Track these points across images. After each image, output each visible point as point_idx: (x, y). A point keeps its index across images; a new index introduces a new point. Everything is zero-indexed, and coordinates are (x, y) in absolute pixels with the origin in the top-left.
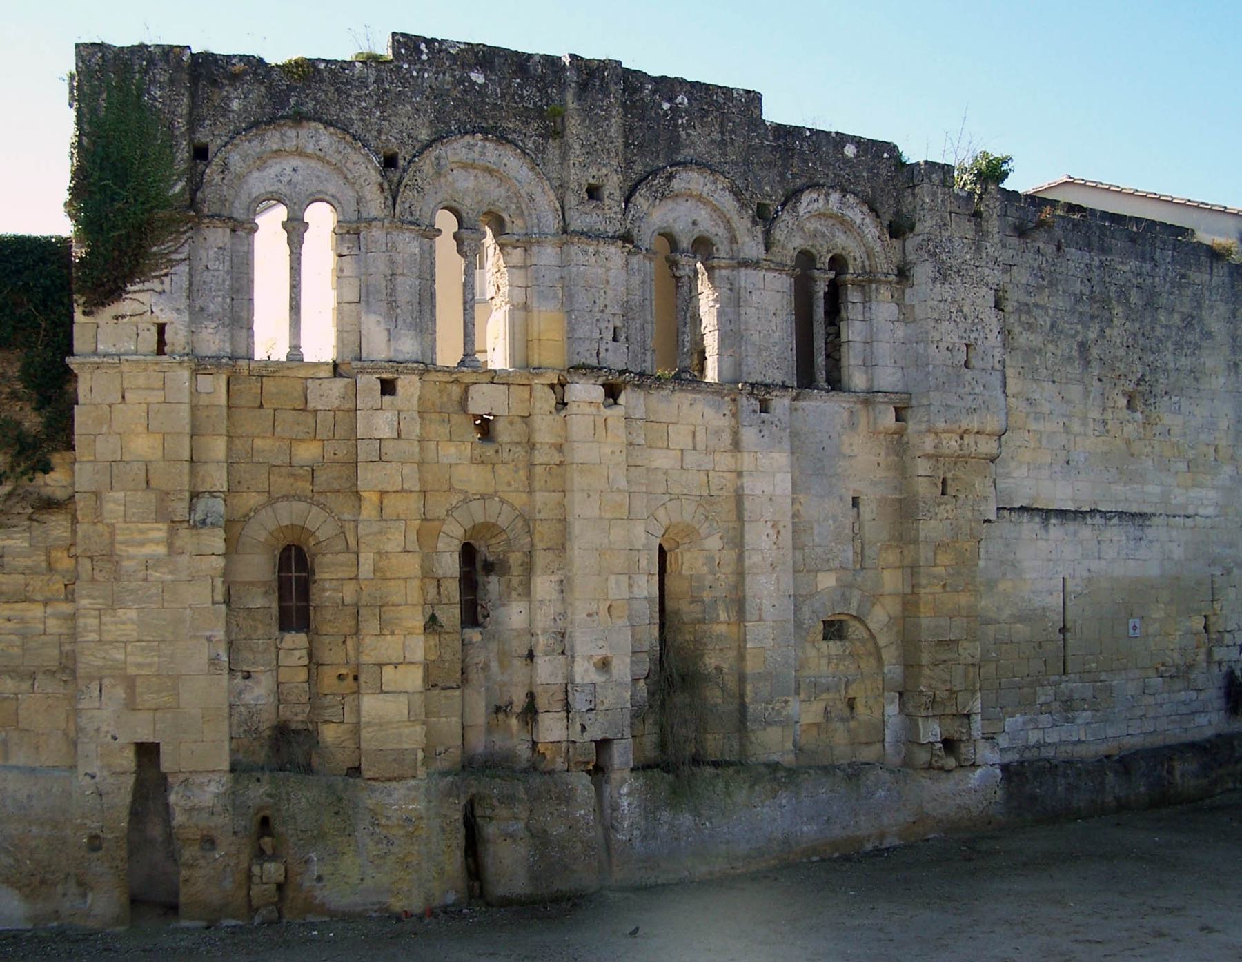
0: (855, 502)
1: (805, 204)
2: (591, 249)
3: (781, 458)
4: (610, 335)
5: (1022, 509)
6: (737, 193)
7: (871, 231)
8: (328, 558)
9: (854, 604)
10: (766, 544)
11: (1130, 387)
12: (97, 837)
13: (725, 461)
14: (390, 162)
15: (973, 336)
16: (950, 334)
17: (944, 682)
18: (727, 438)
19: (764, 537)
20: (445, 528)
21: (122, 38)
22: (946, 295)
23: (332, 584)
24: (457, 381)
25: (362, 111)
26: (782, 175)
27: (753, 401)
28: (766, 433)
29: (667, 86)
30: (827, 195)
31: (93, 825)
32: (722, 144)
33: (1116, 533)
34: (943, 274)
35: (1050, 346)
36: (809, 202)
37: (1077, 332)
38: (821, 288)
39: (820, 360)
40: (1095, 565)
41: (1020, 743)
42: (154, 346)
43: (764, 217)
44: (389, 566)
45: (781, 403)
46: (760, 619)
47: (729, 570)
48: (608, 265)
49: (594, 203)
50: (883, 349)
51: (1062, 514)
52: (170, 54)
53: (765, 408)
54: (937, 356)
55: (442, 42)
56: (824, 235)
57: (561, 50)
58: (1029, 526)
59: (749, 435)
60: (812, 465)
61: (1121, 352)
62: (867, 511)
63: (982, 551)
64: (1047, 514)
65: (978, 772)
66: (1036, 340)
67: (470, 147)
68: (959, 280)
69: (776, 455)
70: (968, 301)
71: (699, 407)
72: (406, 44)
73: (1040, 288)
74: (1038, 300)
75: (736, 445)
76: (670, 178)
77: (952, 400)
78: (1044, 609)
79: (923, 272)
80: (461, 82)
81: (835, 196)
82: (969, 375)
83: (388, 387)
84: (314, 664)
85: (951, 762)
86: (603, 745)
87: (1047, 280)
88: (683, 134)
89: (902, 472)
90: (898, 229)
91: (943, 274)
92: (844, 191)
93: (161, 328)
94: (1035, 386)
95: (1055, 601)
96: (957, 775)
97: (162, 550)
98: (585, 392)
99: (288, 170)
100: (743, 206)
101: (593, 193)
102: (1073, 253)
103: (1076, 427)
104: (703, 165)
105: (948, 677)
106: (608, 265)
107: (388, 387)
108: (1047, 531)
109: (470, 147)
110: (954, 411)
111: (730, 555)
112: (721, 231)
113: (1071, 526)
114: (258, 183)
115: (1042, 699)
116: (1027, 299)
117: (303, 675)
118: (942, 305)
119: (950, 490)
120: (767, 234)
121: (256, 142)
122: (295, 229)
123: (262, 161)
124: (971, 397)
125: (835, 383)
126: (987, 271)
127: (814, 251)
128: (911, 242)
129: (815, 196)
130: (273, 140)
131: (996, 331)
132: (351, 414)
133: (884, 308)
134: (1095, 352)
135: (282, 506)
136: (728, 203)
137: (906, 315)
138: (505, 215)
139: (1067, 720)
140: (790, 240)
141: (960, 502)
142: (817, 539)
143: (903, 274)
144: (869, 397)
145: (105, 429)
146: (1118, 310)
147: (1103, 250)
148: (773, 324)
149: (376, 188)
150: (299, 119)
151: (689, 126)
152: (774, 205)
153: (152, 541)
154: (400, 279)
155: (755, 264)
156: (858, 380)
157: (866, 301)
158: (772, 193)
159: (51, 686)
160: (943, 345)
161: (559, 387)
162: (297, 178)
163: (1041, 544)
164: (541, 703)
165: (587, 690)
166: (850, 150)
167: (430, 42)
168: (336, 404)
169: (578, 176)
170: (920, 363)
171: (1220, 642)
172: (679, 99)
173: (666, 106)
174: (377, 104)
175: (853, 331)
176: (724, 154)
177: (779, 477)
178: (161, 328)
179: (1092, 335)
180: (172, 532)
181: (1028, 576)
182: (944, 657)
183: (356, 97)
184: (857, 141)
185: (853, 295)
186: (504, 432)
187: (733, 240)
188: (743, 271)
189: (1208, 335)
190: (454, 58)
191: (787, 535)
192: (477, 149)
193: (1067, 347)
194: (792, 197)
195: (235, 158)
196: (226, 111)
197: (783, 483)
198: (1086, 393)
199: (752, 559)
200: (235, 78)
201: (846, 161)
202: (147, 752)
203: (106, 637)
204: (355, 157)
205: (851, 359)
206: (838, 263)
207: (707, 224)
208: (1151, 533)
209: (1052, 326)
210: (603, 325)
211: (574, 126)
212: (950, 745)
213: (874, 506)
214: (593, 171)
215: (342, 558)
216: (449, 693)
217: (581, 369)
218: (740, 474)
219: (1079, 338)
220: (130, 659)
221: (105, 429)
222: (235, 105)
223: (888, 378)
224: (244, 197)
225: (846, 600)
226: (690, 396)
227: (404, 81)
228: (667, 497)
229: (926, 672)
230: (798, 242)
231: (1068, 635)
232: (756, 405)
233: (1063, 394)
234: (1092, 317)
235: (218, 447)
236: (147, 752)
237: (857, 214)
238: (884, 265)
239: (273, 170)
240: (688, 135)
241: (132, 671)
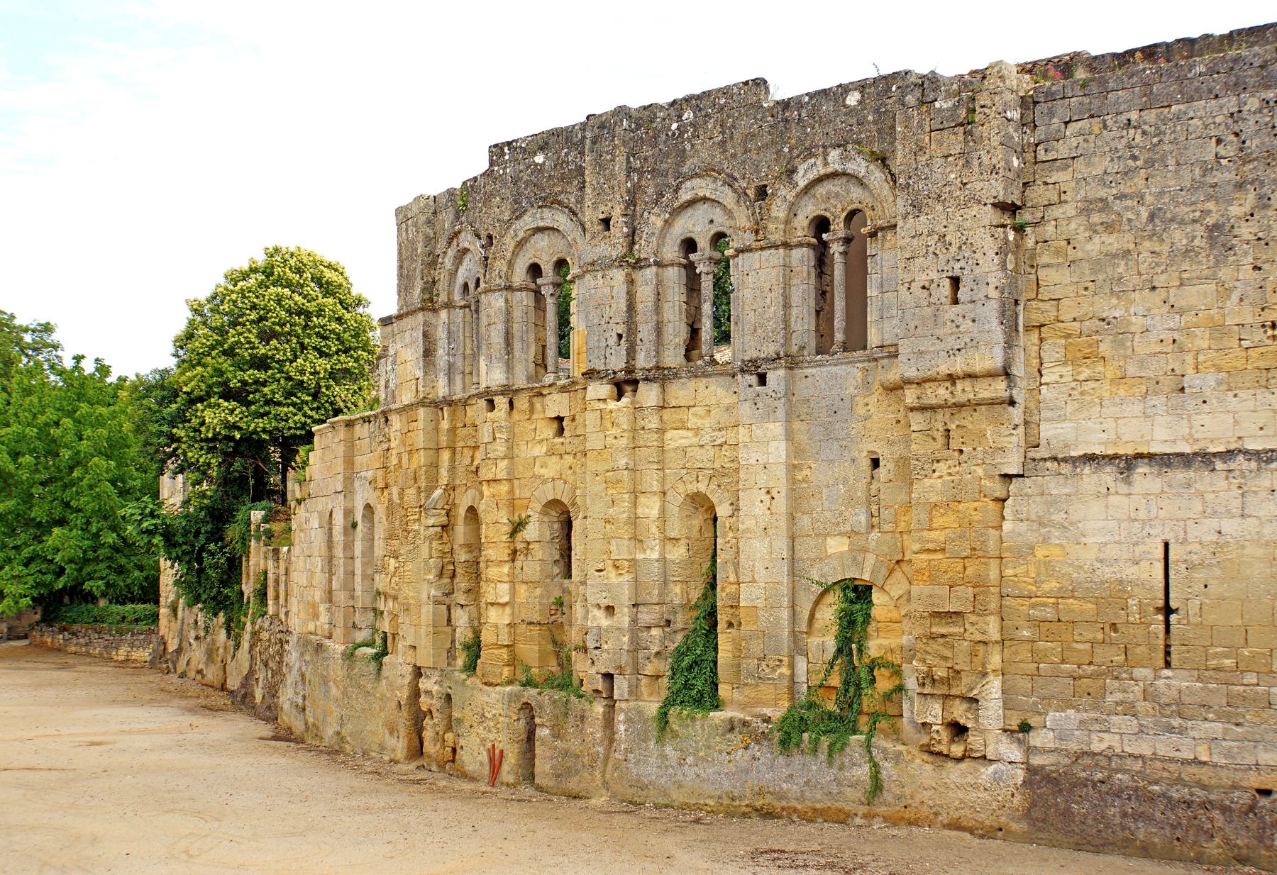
0: (875, 463)
1: (801, 172)
2: (600, 274)
3: (777, 428)
10: (759, 510)
15: (957, 266)
17: (946, 658)
19: (758, 503)
22: (920, 228)
26: (779, 152)
27: (747, 377)
28: (760, 405)
30: (825, 155)
35: (1147, 244)
37: (1206, 213)
41: (1074, 746)
46: (754, 581)
48: (613, 283)
53: (762, 380)
56: (837, 195)
63: (1007, 512)
64: (1127, 463)
66: (1114, 242)
68: (939, 207)
69: (771, 426)
70: (951, 227)
74: (1125, 189)
77: (926, 345)
78: (1121, 582)
81: (834, 154)
88: (688, 147)
94: (1114, 301)
101: (606, 222)
104: (707, 171)
105: (950, 655)
106: (613, 283)
108: (1127, 481)
109: (534, 215)
110: (928, 357)
113: (1180, 475)
116: (1102, 193)
118: (915, 242)
119: (954, 444)
124: (954, 337)
125: (855, 340)
126: (979, 185)
127: (828, 215)
129: (813, 160)
131: (991, 254)
141: (963, 457)
142: (826, 504)
148: (768, 301)
158: (768, 168)
160: (916, 287)
163: (1113, 499)
165: (595, 631)
172: (686, 116)
177: (773, 445)
181: (1089, 540)
182: (943, 631)
192: (538, 216)
197: (778, 452)
201: (851, 111)
209: (1152, 217)
210: (607, 335)
213: (891, 466)
214: (602, 208)
216: (531, 627)
219: (1209, 221)
226: (704, 380)
228: (684, 471)
230: (809, 210)
231: (1173, 617)
232: (753, 379)
233: (1172, 300)
234: (1240, 186)
235: (446, 455)
240: (693, 145)
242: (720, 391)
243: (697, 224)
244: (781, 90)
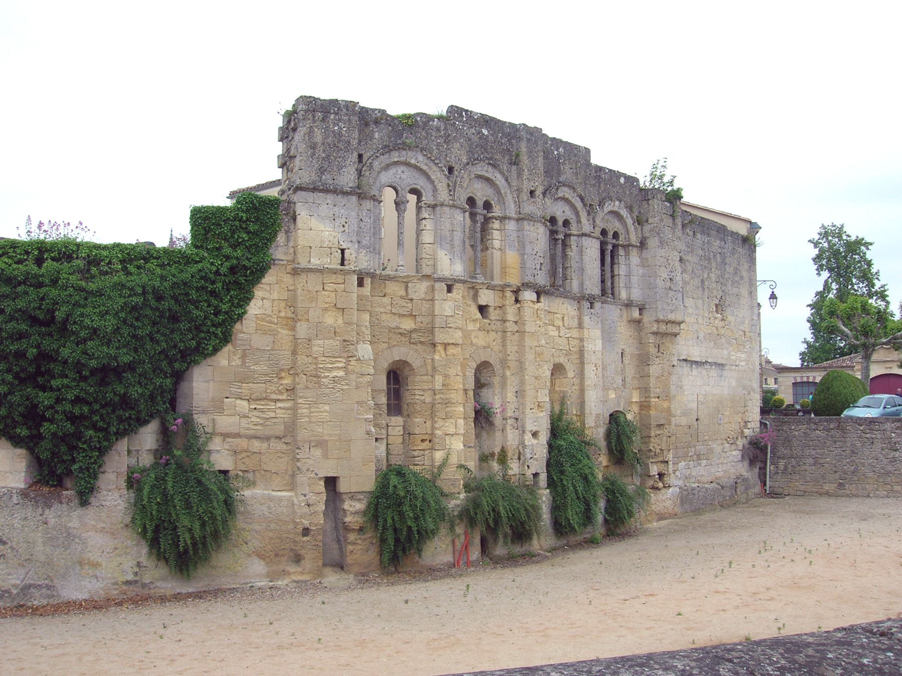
4: (538, 267)
5: (685, 360)
6: (582, 199)
7: (629, 221)
8: (418, 378)
9: (622, 405)
10: (592, 375)
11: (717, 302)
12: (308, 529)
13: (575, 333)
14: (451, 170)
16: (664, 274)
17: (659, 445)
18: (576, 321)
20: (469, 364)
21: (325, 94)
23: (418, 391)
24: (473, 288)
25: (438, 145)
29: (557, 142)
31: (306, 523)
32: (576, 174)
33: (714, 372)
34: (662, 243)
36: (608, 207)
38: (610, 247)
39: (609, 284)
40: (707, 388)
42: (340, 262)
43: (591, 210)
44: (446, 382)
45: (598, 305)
47: (577, 387)
49: (533, 200)
50: (635, 280)
51: (696, 362)
52: (350, 106)
54: (660, 283)
55: (471, 112)
57: (516, 120)
58: (686, 368)
59: (586, 319)
60: (608, 337)
61: (714, 285)
62: (627, 360)
65: (671, 490)
67: (482, 166)
71: (565, 305)
72: (456, 112)
73: (688, 252)
75: (580, 326)
76: (557, 189)
79: (653, 242)
80: (479, 133)
81: (617, 203)
82: (671, 293)
83: (450, 289)
84: (408, 434)
85: (661, 485)
86: (536, 475)
87: (691, 248)
89: (641, 343)
90: (640, 222)
91: (662, 243)
92: (620, 201)
93: (343, 251)
95: (694, 405)
96: (663, 491)
97: (341, 373)
98: (528, 295)
99: (400, 172)
100: (585, 205)
102: (699, 236)
103: (700, 321)
107: (450, 289)
111: (576, 381)
112: (574, 217)
113: (699, 369)
114: (385, 177)
115: (691, 454)
117: (401, 440)
119: (661, 351)
120: (593, 219)
121: (386, 156)
122: (399, 205)
123: (387, 167)
128: (647, 228)
130: (395, 156)
132: (431, 302)
133: (635, 258)
134: (706, 283)
135: (395, 349)
136: (579, 204)
137: (644, 264)
138: (492, 203)
139: (700, 464)
140: (600, 224)
143: (643, 245)
144: (629, 305)
145: (314, 305)
146: (714, 265)
147: (709, 235)
149: (445, 185)
150: (405, 147)
151: (564, 163)
152: (595, 203)
153: (339, 368)
154: (455, 233)
155: (589, 236)
156: (624, 295)
157: (627, 254)
159: (281, 446)
161: (516, 292)
162: (404, 176)
164: (510, 454)
166: (622, 180)
167: (467, 111)
168: (423, 296)
169: (527, 186)
170: (651, 287)
171: (745, 427)
173: (556, 153)
174: (445, 142)
175: (621, 270)
176: (577, 179)
178: (343, 251)
179: (706, 276)
180: (348, 363)
183: (436, 137)
184: (624, 175)
185: (621, 252)
186: (493, 314)
187: (579, 221)
188: (584, 238)
189: (742, 278)
190: (475, 120)
191: (600, 369)
192: (485, 168)
193: (697, 282)
194: (601, 204)
195: (376, 164)
196: (372, 138)
198: (704, 304)
199: (588, 382)
200: (377, 122)
201: (621, 185)
202: (331, 482)
203: (313, 420)
204: (435, 168)
205: (621, 283)
206: (616, 235)
207: (569, 215)
208: (725, 373)
211: (525, 159)
212: (661, 475)
215: (425, 378)
217: (526, 285)
218: (582, 340)
220: (325, 432)
221: (314, 305)
222: (376, 135)
223: (636, 294)
224: (378, 185)
225: (619, 404)
227: (457, 130)
229: (652, 439)
236: (331, 482)
237: (624, 213)
238: (634, 239)
239: (392, 171)
241: (326, 438)
242: (569, 307)
243: (561, 212)
244: (595, 160)
